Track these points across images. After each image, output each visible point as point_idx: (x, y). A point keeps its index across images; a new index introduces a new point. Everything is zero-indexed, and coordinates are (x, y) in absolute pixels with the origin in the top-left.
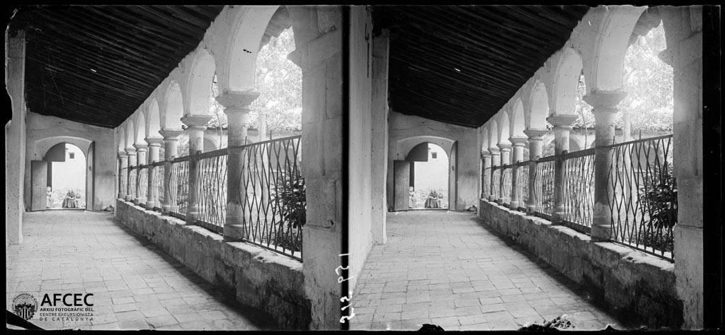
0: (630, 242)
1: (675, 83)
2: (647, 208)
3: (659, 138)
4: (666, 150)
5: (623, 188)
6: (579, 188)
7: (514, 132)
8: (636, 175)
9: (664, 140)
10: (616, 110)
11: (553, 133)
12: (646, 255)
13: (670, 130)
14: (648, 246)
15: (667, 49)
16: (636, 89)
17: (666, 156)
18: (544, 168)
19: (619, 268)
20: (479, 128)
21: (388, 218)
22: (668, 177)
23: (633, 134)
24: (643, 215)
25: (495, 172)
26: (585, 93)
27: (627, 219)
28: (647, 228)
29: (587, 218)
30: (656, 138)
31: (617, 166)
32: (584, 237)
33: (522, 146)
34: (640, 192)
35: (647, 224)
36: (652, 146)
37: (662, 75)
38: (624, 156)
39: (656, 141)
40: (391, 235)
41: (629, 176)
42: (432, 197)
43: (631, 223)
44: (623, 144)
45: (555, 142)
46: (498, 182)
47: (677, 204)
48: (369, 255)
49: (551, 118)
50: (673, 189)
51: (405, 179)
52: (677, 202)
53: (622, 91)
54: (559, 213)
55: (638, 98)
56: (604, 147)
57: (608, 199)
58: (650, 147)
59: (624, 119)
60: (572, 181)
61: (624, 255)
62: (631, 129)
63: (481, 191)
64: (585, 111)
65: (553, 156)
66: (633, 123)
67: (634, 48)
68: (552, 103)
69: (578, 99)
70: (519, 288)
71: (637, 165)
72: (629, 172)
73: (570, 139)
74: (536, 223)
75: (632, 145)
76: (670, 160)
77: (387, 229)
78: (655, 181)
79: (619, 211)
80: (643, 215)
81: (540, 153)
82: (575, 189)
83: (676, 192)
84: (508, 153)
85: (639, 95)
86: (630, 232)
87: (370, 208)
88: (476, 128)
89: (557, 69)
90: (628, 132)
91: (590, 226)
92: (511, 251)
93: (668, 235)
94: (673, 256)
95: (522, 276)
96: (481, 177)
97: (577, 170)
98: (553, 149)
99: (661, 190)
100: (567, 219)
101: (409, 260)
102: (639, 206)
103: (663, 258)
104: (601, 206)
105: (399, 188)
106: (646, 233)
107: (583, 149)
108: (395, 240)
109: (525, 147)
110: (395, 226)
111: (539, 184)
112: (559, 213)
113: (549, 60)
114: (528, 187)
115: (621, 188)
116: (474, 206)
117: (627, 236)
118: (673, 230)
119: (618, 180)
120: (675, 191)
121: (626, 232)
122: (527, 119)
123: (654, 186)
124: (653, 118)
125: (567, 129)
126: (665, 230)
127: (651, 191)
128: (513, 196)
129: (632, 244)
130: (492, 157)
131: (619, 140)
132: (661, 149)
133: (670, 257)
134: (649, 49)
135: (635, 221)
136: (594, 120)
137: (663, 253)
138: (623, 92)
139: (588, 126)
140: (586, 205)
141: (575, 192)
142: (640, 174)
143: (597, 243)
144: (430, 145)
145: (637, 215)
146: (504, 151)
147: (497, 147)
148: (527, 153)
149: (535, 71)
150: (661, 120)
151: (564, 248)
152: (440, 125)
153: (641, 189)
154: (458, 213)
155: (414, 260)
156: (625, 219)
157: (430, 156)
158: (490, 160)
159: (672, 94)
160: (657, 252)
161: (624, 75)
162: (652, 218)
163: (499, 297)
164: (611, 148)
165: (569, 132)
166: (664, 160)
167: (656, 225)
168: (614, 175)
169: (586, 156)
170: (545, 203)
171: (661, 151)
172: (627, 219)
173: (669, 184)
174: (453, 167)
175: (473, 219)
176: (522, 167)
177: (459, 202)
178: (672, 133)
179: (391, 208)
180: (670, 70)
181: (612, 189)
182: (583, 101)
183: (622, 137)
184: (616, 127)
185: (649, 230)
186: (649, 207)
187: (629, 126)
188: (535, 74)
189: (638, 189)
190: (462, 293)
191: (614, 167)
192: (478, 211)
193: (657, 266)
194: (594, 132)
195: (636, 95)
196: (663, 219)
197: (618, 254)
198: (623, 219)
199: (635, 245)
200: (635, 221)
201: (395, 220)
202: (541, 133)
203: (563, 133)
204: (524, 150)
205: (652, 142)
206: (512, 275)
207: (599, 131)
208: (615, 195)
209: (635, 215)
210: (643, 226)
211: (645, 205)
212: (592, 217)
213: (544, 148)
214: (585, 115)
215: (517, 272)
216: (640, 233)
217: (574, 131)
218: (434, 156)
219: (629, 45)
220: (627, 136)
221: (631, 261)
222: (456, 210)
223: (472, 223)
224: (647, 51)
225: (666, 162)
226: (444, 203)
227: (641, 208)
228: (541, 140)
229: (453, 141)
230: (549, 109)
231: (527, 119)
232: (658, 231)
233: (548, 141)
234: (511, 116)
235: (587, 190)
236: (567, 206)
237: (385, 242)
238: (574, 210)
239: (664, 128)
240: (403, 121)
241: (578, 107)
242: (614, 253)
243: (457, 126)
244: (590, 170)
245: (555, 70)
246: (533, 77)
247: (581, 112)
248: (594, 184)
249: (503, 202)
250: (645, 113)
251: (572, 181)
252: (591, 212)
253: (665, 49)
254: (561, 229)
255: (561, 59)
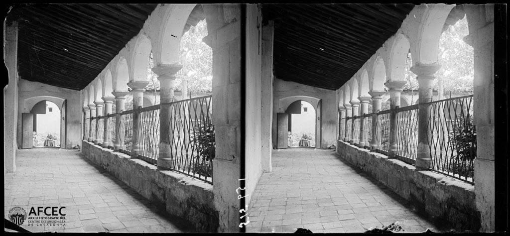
2: (455, 147)
5: (438, 132)
7: (362, 93)
8: (448, 123)
9: (467, 99)
10: (434, 78)
11: (389, 93)
12: (455, 180)
13: (471, 91)
14: (456, 173)
17: (468, 110)
18: (383, 118)
20: (337, 90)
22: (470, 125)
23: (445, 94)
24: (452, 151)
27: (441, 154)
29: (413, 154)
30: (461, 97)
31: (434, 117)
34: (450, 135)
37: (465, 53)
39: (462, 99)
41: (443, 124)
45: (391, 100)
46: (351, 128)
47: (476, 144)
49: (388, 83)
54: (393, 150)
57: (428, 140)
58: (457, 104)
59: (439, 84)
63: (338, 134)
66: (446, 86)
68: (388, 72)
70: (365, 203)
72: (442, 121)
76: (471, 113)
78: (461, 127)
80: (452, 151)
83: (476, 135)
84: (358, 108)
89: (392, 48)
90: (442, 93)
92: (360, 177)
93: (470, 165)
94: (473, 180)
95: (367, 194)
96: (338, 125)
98: (389, 105)
99: (465, 134)
100: (399, 154)
102: (450, 145)
103: (466, 181)
106: (454, 164)
107: (410, 105)
109: (369, 104)
112: (393, 150)
113: (386, 42)
114: (371, 132)
116: (333, 145)
118: (473, 162)
121: (441, 163)
123: (460, 131)
125: (399, 91)
126: (468, 162)
129: (445, 172)
130: (346, 111)
133: (472, 181)
135: (446, 155)
136: (418, 84)
137: (466, 178)
139: (414, 89)
140: (412, 144)
142: (450, 123)
143: (420, 171)
144: (302, 102)
145: (448, 151)
146: (355, 106)
149: (377, 50)
153: (451, 133)
154: (322, 150)
157: (302, 110)
158: (345, 113)
159: (473, 66)
161: (439, 53)
162: (459, 153)
163: (351, 209)
164: (430, 105)
165: (400, 93)
166: (467, 113)
167: (461, 158)
168: (432, 123)
170: (384, 143)
175: (332, 154)
177: (323, 143)
181: (431, 133)
182: (410, 71)
183: (438, 96)
184: (433, 89)
185: (456, 162)
186: (456, 146)
189: (449, 133)
190: (325, 207)
194: (418, 93)
199: (447, 173)
204: (369, 106)
205: (458, 100)
206: (360, 194)
207: (422, 92)
209: (446, 152)
210: (452, 160)
211: (454, 145)
212: (416, 153)
213: (383, 104)
215: (364, 191)
216: (450, 164)
218: (306, 110)
223: (332, 157)
224: (455, 36)
227: (451, 146)
228: (381, 99)
230: (386, 77)
232: (463, 162)
233: (385, 99)
234: (360, 82)
235: (413, 134)
239: (467, 90)
242: (432, 178)
243: (321, 89)
244: (415, 119)
245: (390, 50)
246: (375, 54)
248: (418, 130)
249: (354, 143)
252: (416, 149)
255: (395, 42)
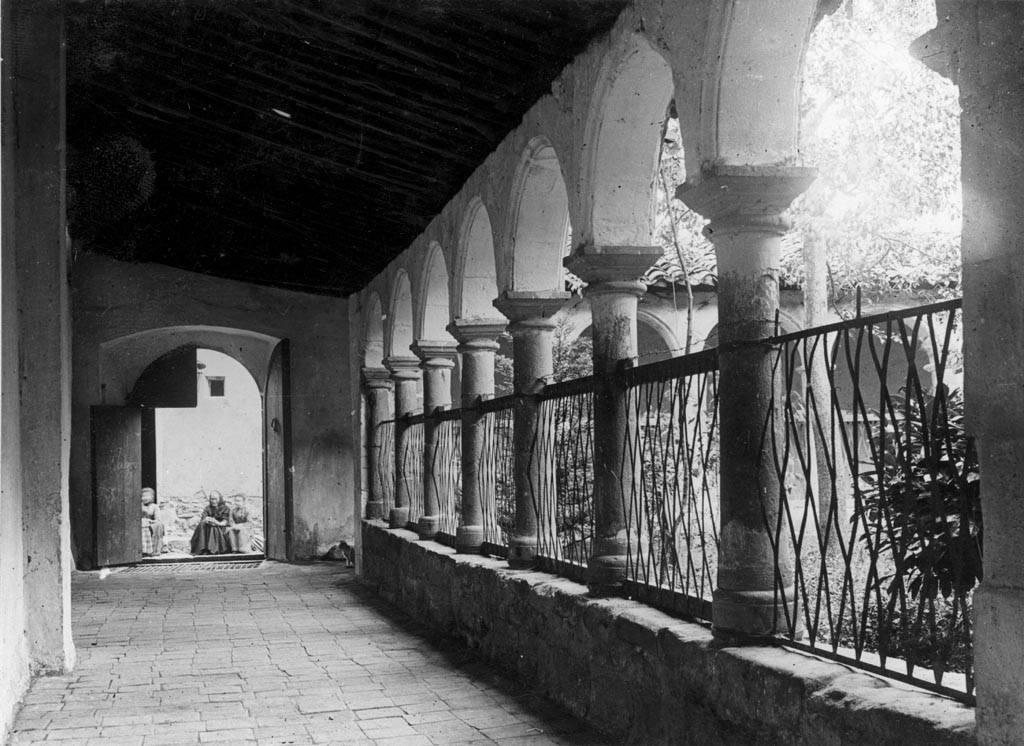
0: (834, 643)
1: (964, 134)
2: (884, 536)
3: (918, 312)
4: (940, 349)
5: (807, 473)
6: (670, 476)
8: (850, 431)
9: (935, 316)
10: (780, 229)
12: (887, 685)
13: (953, 285)
14: (894, 655)
15: (939, 26)
16: (842, 158)
17: (940, 369)
18: (562, 415)
19: (805, 726)
20: (353, 296)
21: (79, 591)
22: (950, 435)
23: (835, 302)
24: (874, 557)
25: (407, 434)
26: (682, 176)
27: (824, 572)
28: (887, 597)
31: (788, 405)
32: (690, 632)
33: (490, 349)
34: (863, 485)
35: (886, 585)
36: (897, 339)
37: (923, 111)
38: (809, 371)
39: (910, 322)
40: (87, 641)
41: (828, 434)
42: (213, 520)
43: (835, 587)
44: (805, 334)
45: (592, 332)
46: (418, 466)
47: (978, 520)
48: (21, 708)
49: (582, 259)
50: (966, 472)
51: (129, 467)
52: (979, 513)
53: (798, 164)
54: (611, 558)
55: (850, 187)
56: (746, 344)
57: (764, 510)
58: (889, 342)
59: (806, 255)
60: (648, 457)
61: (818, 686)
62: (831, 285)
63: (364, 495)
64: (684, 235)
65: (586, 379)
67: (835, 27)
68: (580, 214)
69: (660, 195)
71: (851, 400)
72: (826, 422)
73: (638, 321)
74: (540, 591)
75: (832, 336)
76: (954, 381)
77: (74, 625)
78: (911, 449)
79: (798, 547)
80: (874, 557)
81: (546, 371)
82: (660, 480)
83: (976, 483)
84: (448, 372)
85: (852, 178)
86: (835, 610)
87: (20, 560)
88: (346, 295)
89: (594, 100)
90: (821, 294)
91: (709, 598)
92: (465, 682)
93: (954, 616)
94: (970, 683)
96: (363, 452)
97: (664, 422)
98: (587, 358)
99: (927, 478)
101: (148, 718)
102: (861, 531)
103: (938, 690)
104: (742, 531)
105: (109, 496)
106: (884, 614)
107: (682, 353)
108: (100, 657)
109: (499, 352)
110: (99, 613)
111: (548, 469)
112: (611, 558)
114: (510, 480)
115: (801, 475)
116: (343, 545)
117: (824, 624)
118: (969, 601)
119: (793, 448)
120: (970, 479)
121: (823, 612)
122: (505, 266)
123: (906, 466)
124: (898, 248)
125: (632, 291)
126: (942, 603)
127: (897, 480)
128: (466, 510)
129: (842, 651)
130: (398, 386)
131: (793, 322)
132: (927, 345)
133: (963, 689)
134: (881, 26)
135: (848, 575)
137: (939, 677)
138: (802, 169)
139: (694, 281)
140: (695, 530)
141: (660, 490)
142: (862, 429)
143: (732, 651)
144: (202, 355)
145: (855, 558)
146: (436, 367)
147: (411, 355)
148: (507, 369)
150: (923, 255)
151: (631, 671)
152: (232, 290)
153: (867, 477)
154: (293, 567)
155: (161, 718)
156: (817, 571)
157: (203, 388)
159: (957, 169)
160: (920, 673)
161: (803, 114)
162: (902, 566)
164: (769, 349)
166: (935, 382)
167: (914, 587)
168: (780, 431)
169: (691, 374)
170: (566, 526)
171: (924, 353)
172: (824, 572)
173: (954, 456)
174: (276, 421)
175: (341, 585)
176: (491, 416)
177: (296, 534)
178: (960, 294)
179: (87, 557)
180: (947, 93)
181: (775, 478)
182: (677, 203)
183: (803, 312)
184: (782, 280)
185: (892, 604)
186: (891, 534)
187: (821, 276)
188: (525, 118)
189: (855, 475)
191: (779, 406)
192: (359, 558)
193: (923, 716)
195: (844, 176)
196: (938, 569)
197: (799, 682)
198: (811, 572)
199: (849, 653)
200: (848, 575)
201: (99, 594)
202: (549, 307)
203: (618, 302)
204: (497, 362)
205: (895, 323)
208: (783, 498)
209: (848, 559)
210: (873, 594)
211: (879, 526)
212: (714, 567)
213: (559, 352)
214: (684, 244)
216: (865, 615)
217: (652, 299)
218: (217, 387)
219: (818, 17)
220: (817, 306)
221: (839, 704)
222: (291, 558)
223: (338, 597)
224: (876, 36)
225: (942, 389)
226: (251, 538)
227: (867, 535)
228: (550, 328)
229: (275, 341)
230: (570, 230)
231: (505, 266)
232: (922, 606)
233: (569, 330)
234: (454, 255)
235: (697, 482)
236: (634, 537)
237: (69, 665)
238: (657, 554)
239: (932, 280)
240: (118, 282)
241: (662, 221)
242: (786, 679)
244: (703, 417)
245: (587, 105)
247: (670, 236)
249: (436, 529)
250: (873, 233)
251: (648, 457)
253: (934, 26)
254: (621, 607)
